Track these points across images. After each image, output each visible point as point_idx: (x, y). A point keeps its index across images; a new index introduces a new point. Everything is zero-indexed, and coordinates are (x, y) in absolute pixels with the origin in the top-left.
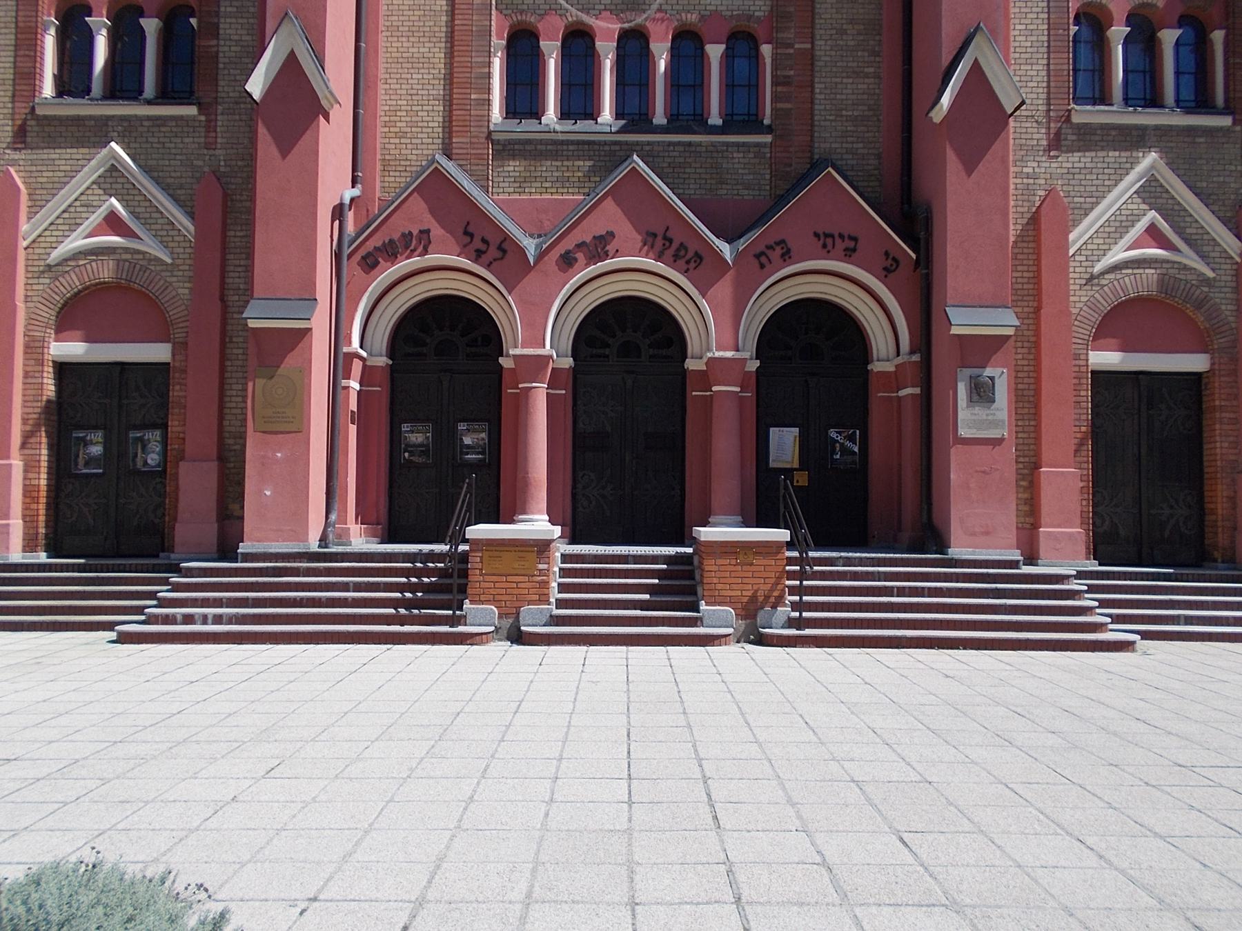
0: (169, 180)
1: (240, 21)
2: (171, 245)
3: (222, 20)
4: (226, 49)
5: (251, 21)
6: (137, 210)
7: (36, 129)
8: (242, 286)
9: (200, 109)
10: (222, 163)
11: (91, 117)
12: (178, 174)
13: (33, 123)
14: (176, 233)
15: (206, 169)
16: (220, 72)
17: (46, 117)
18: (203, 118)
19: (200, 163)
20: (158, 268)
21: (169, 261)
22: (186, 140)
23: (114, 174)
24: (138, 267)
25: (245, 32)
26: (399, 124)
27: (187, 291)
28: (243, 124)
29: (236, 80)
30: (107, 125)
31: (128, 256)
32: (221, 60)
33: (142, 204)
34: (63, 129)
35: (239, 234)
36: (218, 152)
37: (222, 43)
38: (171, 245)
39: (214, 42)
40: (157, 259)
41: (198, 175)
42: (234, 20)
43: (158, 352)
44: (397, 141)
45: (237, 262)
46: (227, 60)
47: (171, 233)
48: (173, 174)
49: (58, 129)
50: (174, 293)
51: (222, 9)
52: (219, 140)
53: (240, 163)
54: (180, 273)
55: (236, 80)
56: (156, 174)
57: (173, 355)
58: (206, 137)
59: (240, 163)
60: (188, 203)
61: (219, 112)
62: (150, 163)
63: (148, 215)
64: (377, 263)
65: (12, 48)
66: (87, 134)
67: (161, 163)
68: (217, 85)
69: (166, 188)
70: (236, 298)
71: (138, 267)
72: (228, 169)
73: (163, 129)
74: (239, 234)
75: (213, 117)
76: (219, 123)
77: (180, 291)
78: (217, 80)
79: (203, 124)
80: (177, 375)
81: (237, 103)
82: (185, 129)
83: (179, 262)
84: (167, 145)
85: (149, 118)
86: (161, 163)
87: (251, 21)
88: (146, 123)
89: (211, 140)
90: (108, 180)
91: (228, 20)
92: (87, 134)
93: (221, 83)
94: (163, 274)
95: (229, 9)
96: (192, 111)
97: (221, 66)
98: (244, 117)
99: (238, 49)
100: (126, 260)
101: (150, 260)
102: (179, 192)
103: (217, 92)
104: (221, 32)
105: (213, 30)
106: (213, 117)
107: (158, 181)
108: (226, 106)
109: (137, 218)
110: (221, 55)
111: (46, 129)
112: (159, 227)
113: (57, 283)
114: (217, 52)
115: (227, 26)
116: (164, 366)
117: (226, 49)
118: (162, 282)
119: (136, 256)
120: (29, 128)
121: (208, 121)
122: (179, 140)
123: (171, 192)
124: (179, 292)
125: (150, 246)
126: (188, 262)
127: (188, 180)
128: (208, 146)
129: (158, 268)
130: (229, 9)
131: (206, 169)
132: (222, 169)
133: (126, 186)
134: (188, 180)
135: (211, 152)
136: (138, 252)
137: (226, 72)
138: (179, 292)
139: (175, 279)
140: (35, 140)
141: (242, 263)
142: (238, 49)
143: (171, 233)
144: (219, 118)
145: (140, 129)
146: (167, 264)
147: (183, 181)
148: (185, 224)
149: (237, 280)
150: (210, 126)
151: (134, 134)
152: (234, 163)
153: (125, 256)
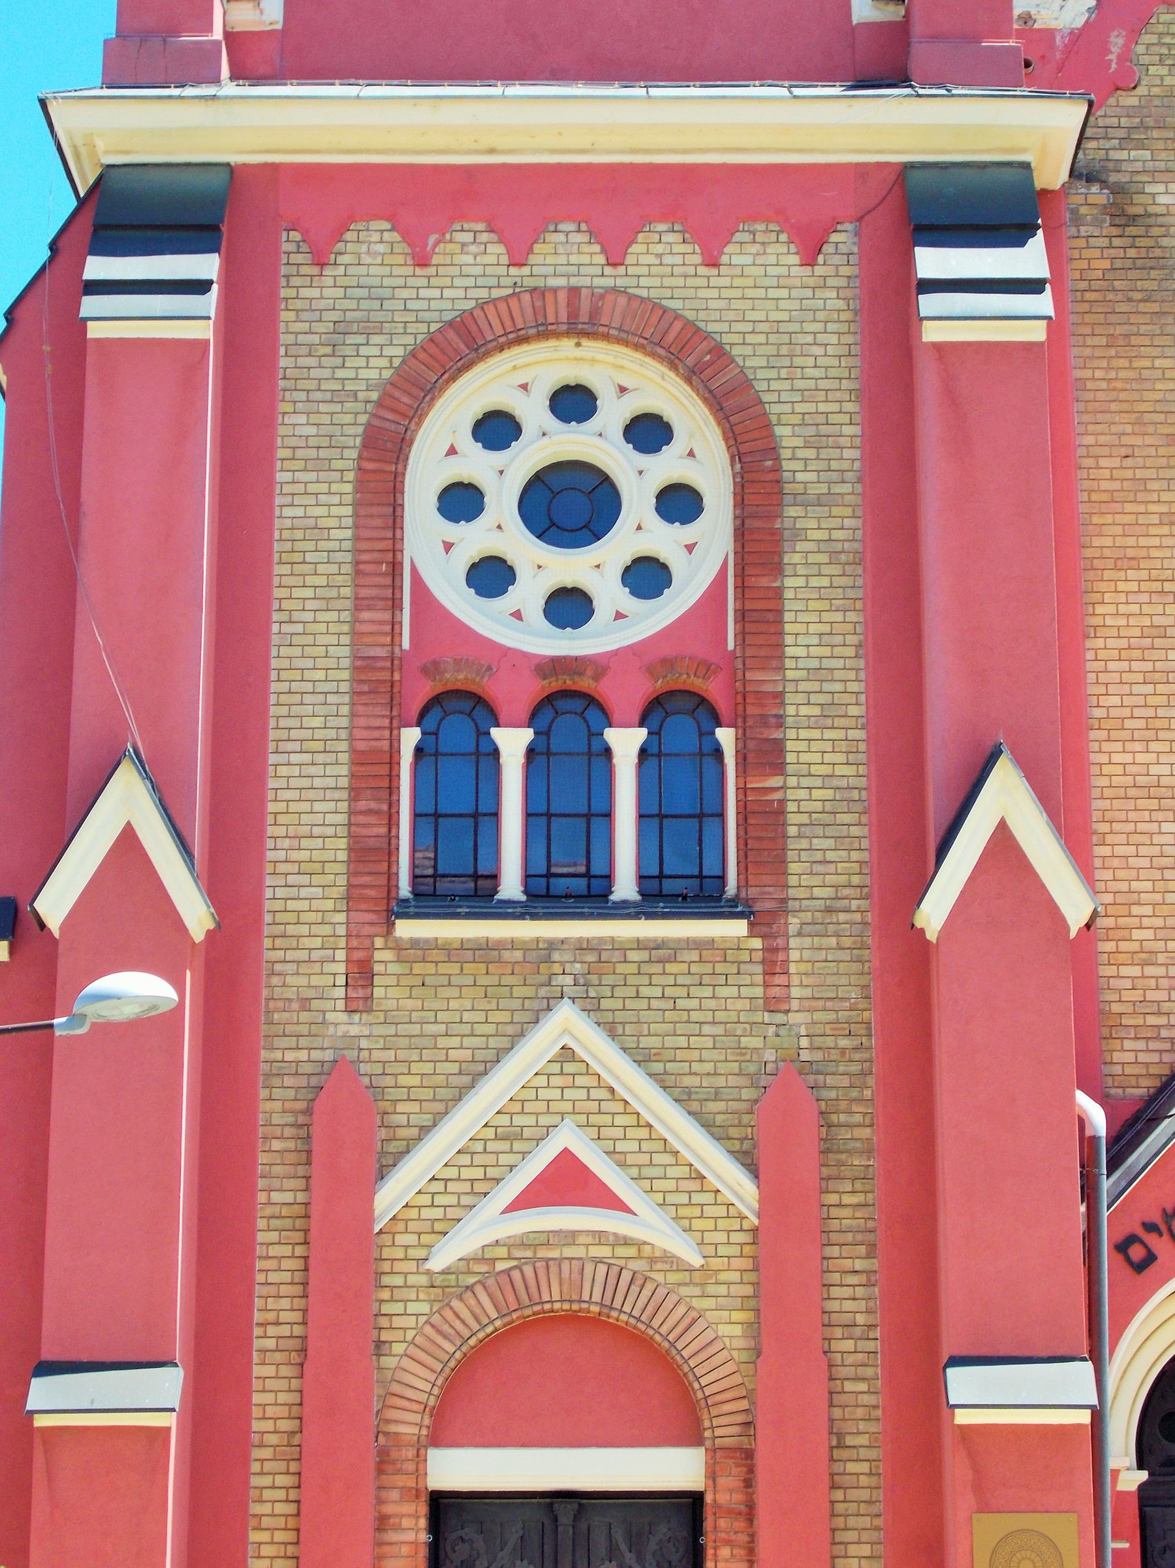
0: (689, 1081)
1: (829, 734)
2: (698, 1224)
3: (791, 734)
4: (803, 794)
5: (852, 734)
6: (621, 1146)
7: (394, 968)
8: (860, 1319)
9: (751, 925)
10: (804, 1042)
11: (513, 944)
12: (709, 1067)
13: (388, 955)
14: (708, 1198)
15: (770, 1055)
16: (791, 844)
17: (415, 943)
18: (757, 943)
19: (757, 1042)
20: (672, 1278)
21: (696, 1261)
22: (723, 992)
23: (569, 1068)
24: (626, 1276)
25: (841, 758)
26: (1137, 934)
27: (737, 1330)
28: (845, 955)
29: (825, 862)
30: (548, 960)
31: (604, 1252)
32: (792, 818)
33: (631, 1133)
34: (454, 968)
35: (847, 1199)
36: (794, 1018)
37: (792, 781)
38: (698, 1224)
39: (775, 781)
40: (669, 1260)
41: (752, 1068)
42: (816, 734)
43: (672, 1468)
44: (1135, 971)
45: (848, 1264)
46: (804, 819)
47: (697, 1198)
48: (696, 1067)
49: (443, 968)
50: (709, 1335)
51: (791, 710)
52: (795, 992)
53: (843, 1042)
54: (723, 1290)
55: (825, 862)
56: (658, 1067)
57: (712, 1474)
58: (766, 985)
59: (843, 1042)
60: (733, 1132)
61: (792, 930)
62: (645, 1042)
63: (644, 1159)
64: (1150, 1258)
65: (345, 795)
66: (506, 980)
67: (669, 1042)
68: (785, 873)
69: (683, 1098)
70: (849, 1345)
71: (626, 1276)
72: (818, 1056)
73: (671, 968)
74: (847, 1199)
75: (780, 942)
76: (794, 955)
77: (723, 1330)
78: (784, 862)
79: (758, 956)
80: (722, 1523)
81: (829, 910)
82: (720, 968)
83: (715, 1263)
84: (681, 1003)
85: (640, 944)
86: (669, 1042)
87: (852, 734)
88: (633, 956)
89: (775, 992)
90: (556, 1081)
91: (803, 734)
92: (506, 980)
93: (793, 868)
94: (684, 1291)
95: (804, 710)
96: (737, 928)
97: (792, 831)
98: (847, 942)
99: (829, 794)
100: (598, 1261)
101: (652, 1260)
102: (713, 1106)
103: (786, 886)
104: (790, 758)
105: (766, 755)
106: (780, 942)
107: (662, 1081)
108: (808, 917)
109: (622, 1165)
110: (791, 807)
111: (418, 968)
112: (670, 1185)
113: (448, 1314)
114: (782, 802)
115: (803, 746)
116: (689, 1506)
117: (803, 794)
118: (681, 1310)
119: (621, 1251)
120: (378, 968)
121: (769, 950)
122: (708, 991)
123: (695, 1106)
124: (717, 1333)
125: (650, 1225)
126: (737, 1263)
127: (732, 1080)
128: (772, 1005)
129: (672, 1278)
130: (804, 710)
131: (770, 1055)
132: (805, 1056)
133: (595, 1094)
134: (732, 1080)
135: (779, 1018)
136: (626, 1242)
137: (804, 844)
138: (717, 1333)
139: (709, 1303)
140: (392, 992)
141: (859, 1265)
142: (829, 794)
143: (697, 1198)
144: (793, 943)
145: (621, 968)
146: (692, 1270)
147: (720, 1081)
148: (739, 1187)
149: (848, 1305)
150: (773, 964)
151: (608, 980)
152: (830, 1041)
153: (595, 1251)
